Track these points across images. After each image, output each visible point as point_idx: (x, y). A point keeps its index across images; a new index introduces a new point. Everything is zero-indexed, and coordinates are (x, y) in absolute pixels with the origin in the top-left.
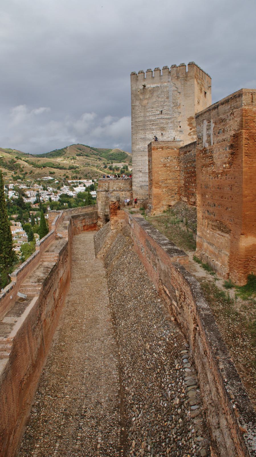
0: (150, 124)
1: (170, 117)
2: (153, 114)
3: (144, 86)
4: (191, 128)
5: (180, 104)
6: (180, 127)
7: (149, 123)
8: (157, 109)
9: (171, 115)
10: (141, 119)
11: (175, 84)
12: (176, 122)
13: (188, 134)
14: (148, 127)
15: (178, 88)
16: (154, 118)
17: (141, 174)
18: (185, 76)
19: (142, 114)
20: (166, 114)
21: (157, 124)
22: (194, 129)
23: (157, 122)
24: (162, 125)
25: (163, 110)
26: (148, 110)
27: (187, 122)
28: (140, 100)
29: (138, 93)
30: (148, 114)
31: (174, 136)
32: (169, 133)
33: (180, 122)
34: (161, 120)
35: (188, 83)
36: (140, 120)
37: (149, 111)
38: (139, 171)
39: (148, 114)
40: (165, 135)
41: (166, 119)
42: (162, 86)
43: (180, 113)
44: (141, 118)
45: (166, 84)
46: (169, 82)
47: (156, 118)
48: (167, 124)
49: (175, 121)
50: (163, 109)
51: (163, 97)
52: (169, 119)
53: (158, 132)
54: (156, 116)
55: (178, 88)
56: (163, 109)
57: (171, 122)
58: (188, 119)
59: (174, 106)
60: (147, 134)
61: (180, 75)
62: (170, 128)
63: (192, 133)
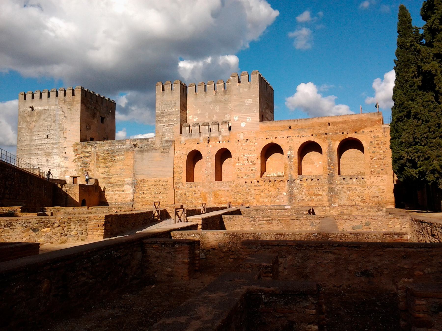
0: (36, 149)
1: (56, 142)
2: (39, 138)
3: (32, 108)
4: (76, 154)
5: (66, 129)
6: (65, 153)
7: (34, 147)
8: (43, 133)
9: (57, 140)
10: (27, 143)
11: (62, 108)
12: (62, 148)
13: (72, 160)
14: (34, 152)
15: (64, 113)
16: (40, 142)
18: (72, 100)
19: (28, 138)
20: (52, 138)
21: (43, 149)
22: (79, 156)
23: (42, 147)
24: (48, 150)
25: (49, 135)
26: (35, 133)
27: (72, 148)
28: (28, 122)
29: (26, 115)
30: (34, 138)
31: (59, 163)
32: (55, 159)
33: (65, 148)
34: (47, 145)
35: (75, 108)
36: (26, 144)
37: (36, 135)
39: (34, 138)
40: (50, 161)
41: (52, 143)
42: (49, 109)
43: (66, 138)
44: (26, 141)
45: (53, 107)
46: (56, 105)
47: (42, 142)
48: (53, 149)
49: (61, 146)
50: (49, 133)
52: (54, 144)
53: (43, 157)
54: (42, 140)
55: (64, 113)
56: (49, 133)
57: (57, 147)
58: (73, 144)
59: (61, 131)
60: (33, 159)
61: (67, 99)
62: (56, 154)
63: (76, 160)
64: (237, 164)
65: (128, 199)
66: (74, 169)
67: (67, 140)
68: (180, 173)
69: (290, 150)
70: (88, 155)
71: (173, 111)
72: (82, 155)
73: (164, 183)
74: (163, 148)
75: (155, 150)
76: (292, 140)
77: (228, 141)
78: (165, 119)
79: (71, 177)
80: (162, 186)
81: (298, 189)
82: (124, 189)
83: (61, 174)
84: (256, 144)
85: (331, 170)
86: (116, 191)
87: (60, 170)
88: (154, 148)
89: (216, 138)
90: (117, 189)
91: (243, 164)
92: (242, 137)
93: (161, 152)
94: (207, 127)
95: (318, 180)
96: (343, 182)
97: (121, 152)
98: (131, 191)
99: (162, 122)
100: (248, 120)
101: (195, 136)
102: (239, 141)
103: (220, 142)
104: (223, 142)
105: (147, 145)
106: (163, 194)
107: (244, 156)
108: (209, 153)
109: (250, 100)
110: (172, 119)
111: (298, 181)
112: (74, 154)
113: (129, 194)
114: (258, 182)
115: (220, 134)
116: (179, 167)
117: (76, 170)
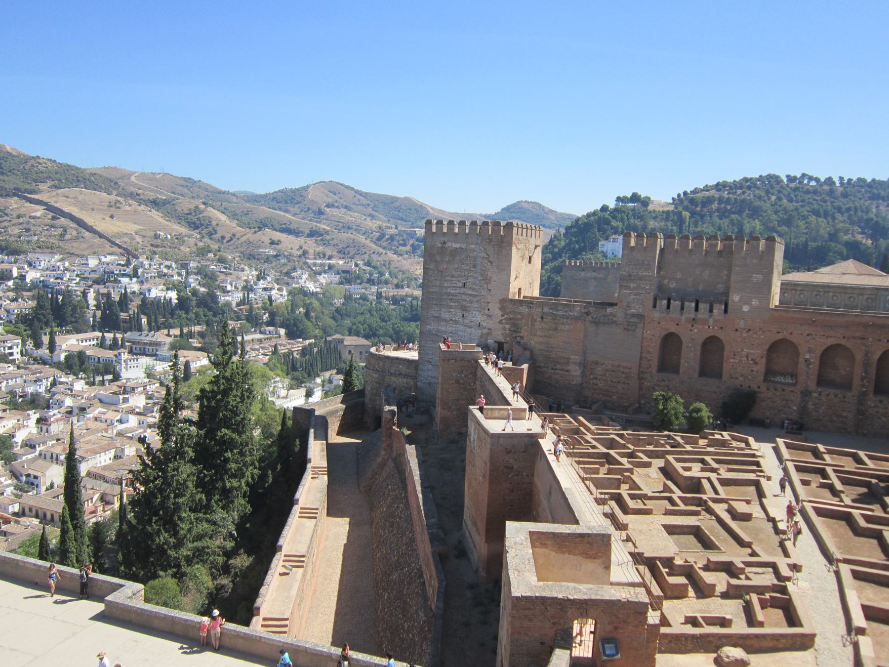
5: (491, 278)
6: (489, 310)
7: (445, 297)
16: (454, 291)
17: (430, 367)
19: (438, 283)
21: (457, 301)
23: (457, 298)
30: (446, 284)
33: (488, 303)
34: (463, 296)
38: (428, 361)
39: (446, 284)
41: (470, 295)
43: (490, 290)
46: (477, 244)
47: (457, 292)
48: (471, 303)
49: (482, 300)
51: (467, 265)
64: (732, 360)
65: (574, 383)
66: (500, 333)
67: (492, 293)
68: (649, 360)
69: (809, 351)
70: (520, 316)
71: (646, 276)
72: (511, 316)
73: (626, 371)
74: (626, 323)
75: (617, 324)
76: (814, 339)
77: (722, 328)
78: (632, 285)
79: (495, 342)
80: (623, 373)
81: (814, 404)
82: (568, 368)
83: (481, 337)
84: (762, 337)
85: (864, 387)
86: (557, 369)
87: (480, 331)
88: (614, 322)
89: (705, 322)
90: (558, 366)
91: (739, 361)
92: (742, 324)
93: (625, 329)
94: (693, 305)
95: (844, 397)
96: (880, 405)
97: (567, 319)
98: (578, 373)
99: (627, 288)
100: (753, 303)
101: (675, 313)
102: (737, 330)
103: (709, 327)
104: (713, 328)
105: (604, 316)
106: (624, 383)
107: (742, 350)
108: (693, 339)
109: (760, 277)
110: (643, 286)
111: (814, 395)
112: (500, 313)
113: (577, 376)
114: (759, 387)
115: (710, 316)
116: (649, 352)
117: (502, 334)
